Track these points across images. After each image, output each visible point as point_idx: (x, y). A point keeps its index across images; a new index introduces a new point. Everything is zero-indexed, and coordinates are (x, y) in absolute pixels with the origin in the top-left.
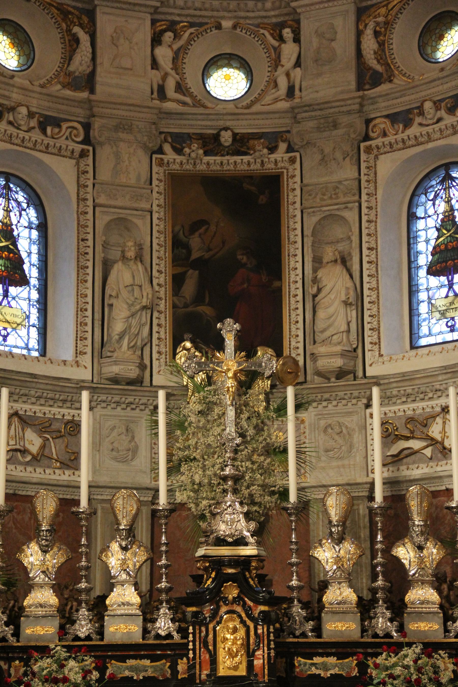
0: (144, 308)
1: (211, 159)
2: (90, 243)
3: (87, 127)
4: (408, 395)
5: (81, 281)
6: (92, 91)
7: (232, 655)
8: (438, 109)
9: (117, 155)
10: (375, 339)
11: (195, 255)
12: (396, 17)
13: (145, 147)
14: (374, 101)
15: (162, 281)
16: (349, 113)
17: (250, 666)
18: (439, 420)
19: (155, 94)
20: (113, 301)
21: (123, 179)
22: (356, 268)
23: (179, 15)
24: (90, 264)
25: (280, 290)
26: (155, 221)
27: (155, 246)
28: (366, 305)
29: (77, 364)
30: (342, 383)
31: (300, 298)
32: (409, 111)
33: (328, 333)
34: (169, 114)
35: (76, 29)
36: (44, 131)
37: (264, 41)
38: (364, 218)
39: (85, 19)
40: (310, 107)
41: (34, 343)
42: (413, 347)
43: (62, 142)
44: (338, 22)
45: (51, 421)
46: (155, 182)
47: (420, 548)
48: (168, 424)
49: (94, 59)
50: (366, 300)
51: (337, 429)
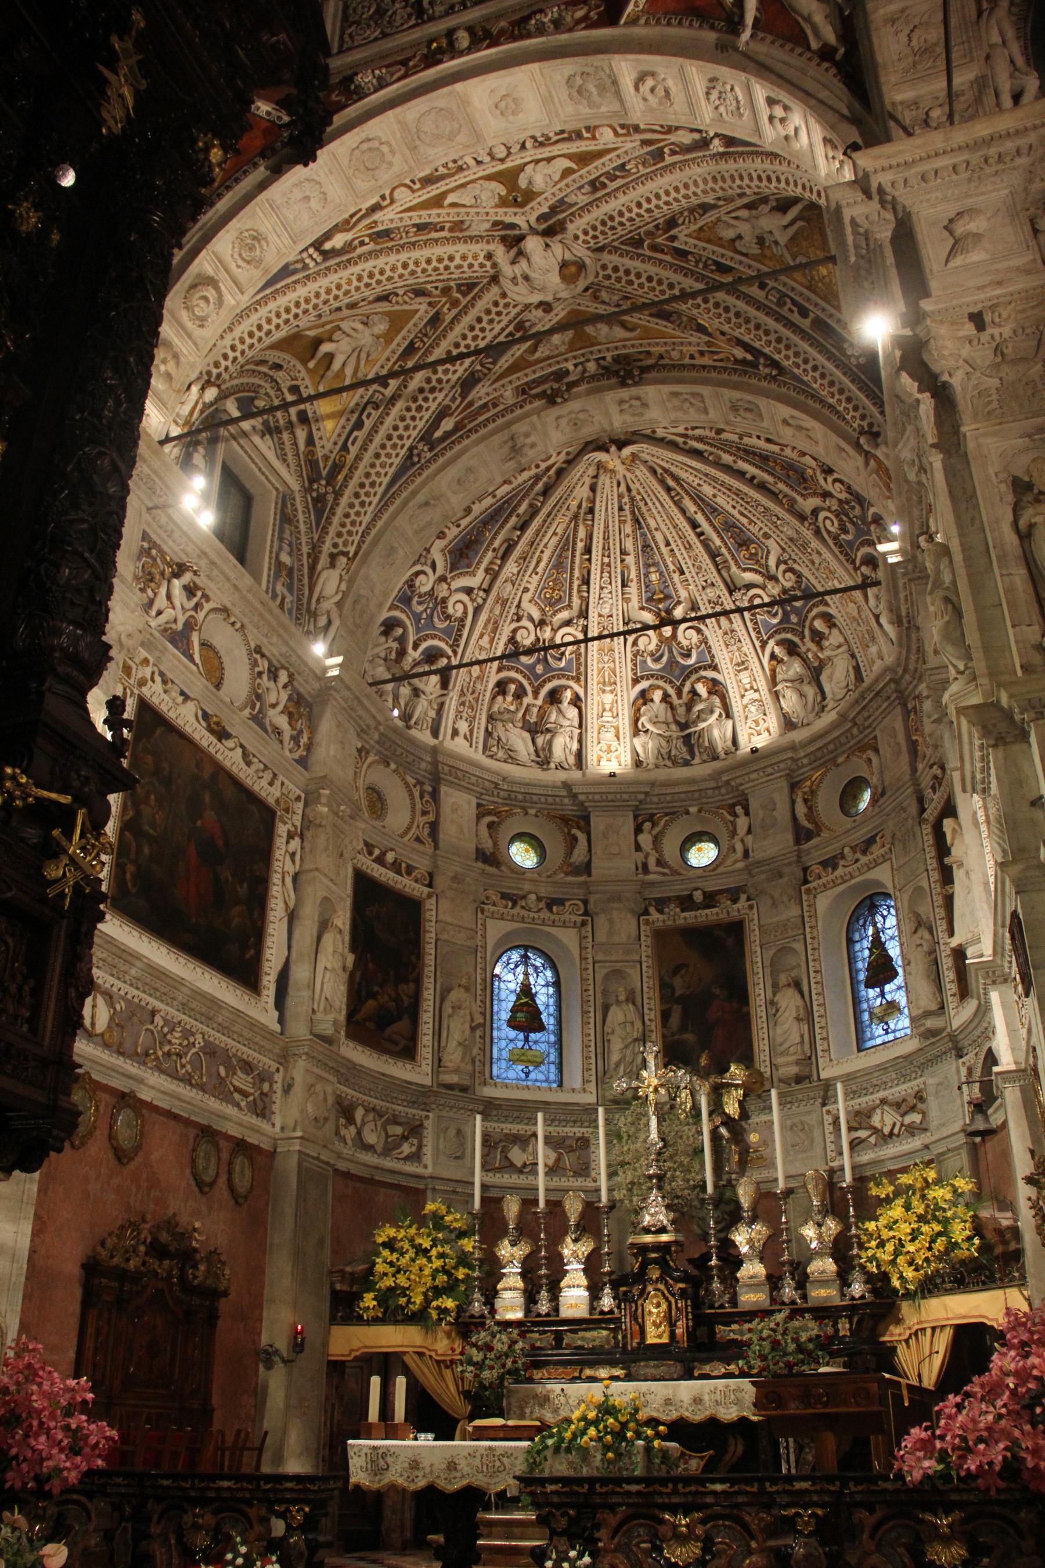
0: (636, 1040)
1: (687, 914)
2: (591, 992)
3: (585, 902)
4: (854, 1092)
5: (585, 1023)
6: (589, 874)
7: (657, 1326)
8: (855, 852)
9: (611, 921)
10: (825, 1047)
11: (678, 993)
12: (818, 786)
13: (633, 912)
14: (808, 852)
15: (652, 1016)
16: (789, 864)
17: (672, 1334)
18: (878, 1111)
20: (611, 1037)
21: (616, 939)
22: (805, 988)
24: (592, 1009)
25: (748, 1014)
26: (644, 968)
27: (645, 989)
28: (816, 1019)
29: (584, 1090)
30: (798, 1087)
31: (764, 1019)
32: (835, 857)
33: (786, 1045)
34: (652, 884)
35: (574, 831)
36: (551, 911)
37: (723, 819)
38: (809, 947)
39: (582, 823)
40: (759, 863)
41: (552, 1077)
42: (860, 1050)
43: (566, 917)
44: (777, 796)
45: (564, 1139)
46: (643, 938)
47: (820, 1225)
48: (607, 1135)
49: (590, 850)
50: (816, 1015)
51: (800, 1127)
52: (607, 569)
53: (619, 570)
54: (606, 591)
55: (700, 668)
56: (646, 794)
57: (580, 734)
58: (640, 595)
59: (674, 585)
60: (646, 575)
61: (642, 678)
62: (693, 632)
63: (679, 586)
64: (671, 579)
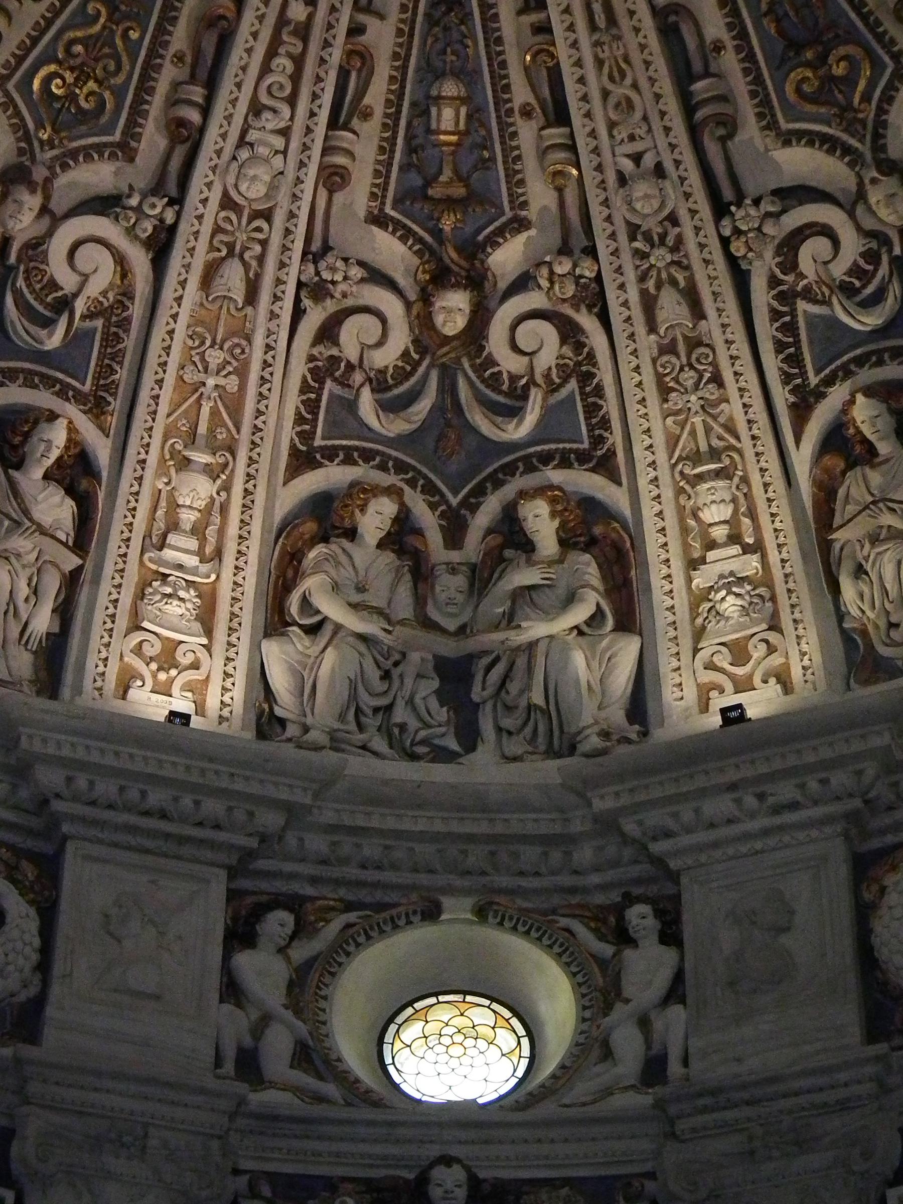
19: (229, 1067)
23: (314, 880)
39: (29, 871)
49: (44, 966)
52: (292, 44)
53: (336, 56)
54: (270, 122)
56: (290, 810)
57: (72, 580)
58: (382, 173)
59: (513, 158)
60: (421, 110)
62: (548, 331)
63: (530, 165)
64: (508, 135)
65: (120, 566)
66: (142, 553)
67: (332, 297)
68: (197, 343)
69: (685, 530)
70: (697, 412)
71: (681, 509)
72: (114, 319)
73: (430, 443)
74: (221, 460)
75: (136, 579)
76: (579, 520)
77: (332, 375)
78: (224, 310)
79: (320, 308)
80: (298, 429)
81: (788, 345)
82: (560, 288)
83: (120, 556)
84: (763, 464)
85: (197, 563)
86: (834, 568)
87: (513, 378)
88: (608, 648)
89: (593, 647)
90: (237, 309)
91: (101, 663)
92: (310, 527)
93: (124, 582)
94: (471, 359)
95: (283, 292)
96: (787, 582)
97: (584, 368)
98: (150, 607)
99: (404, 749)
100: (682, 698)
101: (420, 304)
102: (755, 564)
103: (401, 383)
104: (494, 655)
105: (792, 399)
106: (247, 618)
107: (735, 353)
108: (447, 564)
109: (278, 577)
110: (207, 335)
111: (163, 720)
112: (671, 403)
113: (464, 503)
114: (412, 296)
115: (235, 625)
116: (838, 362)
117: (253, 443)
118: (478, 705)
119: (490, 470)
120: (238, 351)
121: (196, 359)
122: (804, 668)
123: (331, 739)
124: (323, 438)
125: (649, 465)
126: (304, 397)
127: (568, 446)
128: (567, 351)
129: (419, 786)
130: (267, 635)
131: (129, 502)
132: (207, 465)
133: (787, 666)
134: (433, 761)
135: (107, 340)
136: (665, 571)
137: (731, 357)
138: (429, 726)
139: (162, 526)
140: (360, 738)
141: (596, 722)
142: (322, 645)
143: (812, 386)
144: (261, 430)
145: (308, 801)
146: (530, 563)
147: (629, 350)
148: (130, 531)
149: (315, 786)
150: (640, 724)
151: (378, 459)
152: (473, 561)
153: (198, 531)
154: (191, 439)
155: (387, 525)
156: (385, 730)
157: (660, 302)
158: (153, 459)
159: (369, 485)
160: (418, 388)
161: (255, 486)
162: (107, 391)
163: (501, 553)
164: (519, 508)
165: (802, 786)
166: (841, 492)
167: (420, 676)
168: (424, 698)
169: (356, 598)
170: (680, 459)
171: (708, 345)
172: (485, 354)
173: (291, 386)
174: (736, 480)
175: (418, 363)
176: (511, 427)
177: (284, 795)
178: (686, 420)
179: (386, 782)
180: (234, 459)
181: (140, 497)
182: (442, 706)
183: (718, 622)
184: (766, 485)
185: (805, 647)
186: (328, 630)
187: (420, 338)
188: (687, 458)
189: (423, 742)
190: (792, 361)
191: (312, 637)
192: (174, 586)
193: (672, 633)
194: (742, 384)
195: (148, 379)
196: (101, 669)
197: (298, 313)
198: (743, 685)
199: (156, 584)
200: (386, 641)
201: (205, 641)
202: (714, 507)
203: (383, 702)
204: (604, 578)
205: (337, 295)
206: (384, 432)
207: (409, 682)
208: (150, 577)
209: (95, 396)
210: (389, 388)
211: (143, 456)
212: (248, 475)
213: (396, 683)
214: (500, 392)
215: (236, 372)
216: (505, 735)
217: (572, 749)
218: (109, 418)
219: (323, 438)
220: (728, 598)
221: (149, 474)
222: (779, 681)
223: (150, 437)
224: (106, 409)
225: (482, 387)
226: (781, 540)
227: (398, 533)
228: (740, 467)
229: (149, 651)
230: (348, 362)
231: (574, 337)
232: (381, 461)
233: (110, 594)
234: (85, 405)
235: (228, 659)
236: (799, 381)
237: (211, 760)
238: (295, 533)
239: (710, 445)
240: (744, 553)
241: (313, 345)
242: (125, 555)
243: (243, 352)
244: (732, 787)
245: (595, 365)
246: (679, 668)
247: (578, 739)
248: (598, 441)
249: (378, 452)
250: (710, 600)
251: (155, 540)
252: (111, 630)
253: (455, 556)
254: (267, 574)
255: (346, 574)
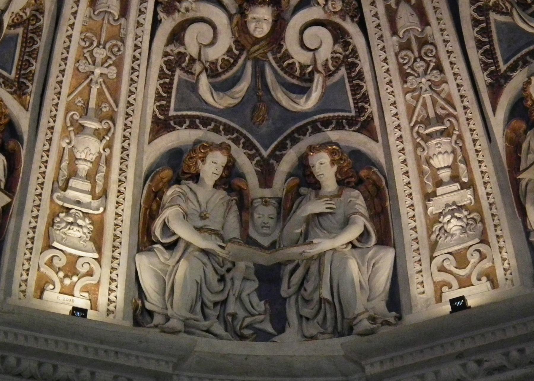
55: (326, 123)
61: (180, 121)
65: (37, 202)
66: (52, 192)
67: (179, 11)
68: (87, 44)
69: (421, 173)
70: (426, 90)
71: (418, 159)
72: (31, 27)
73: (248, 112)
74: (106, 127)
75: (48, 212)
76: (350, 167)
77: (180, 65)
78: (106, 21)
79: (170, 19)
80: (158, 104)
81: (484, 43)
82: (332, 4)
83: (37, 195)
84: (472, 126)
85: (90, 200)
86: (522, 199)
87: (303, 67)
88: (372, 257)
89: (362, 256)
90: (115, 20)
91: (24, 273)
92: (167, 173)
93: (40, 214)
94: (273, 54)
95: (146, 8)
96: (491, 209)
97: (350, 60)
98: (58, 232)
99: (235, 333)
100: (424, 293)
101: (239, 15)
102: (469, 196)
103: (227, 71)
104: (295, 264)
105: (489, 81)
106: (125, 239)
107: (450, 49)
108: (262, 198)
109: (146, 209)
110: (94, 39)
111: (68, 313)
112: (409, 84)
113: (272, 155)
114: (233, 11)
115: (117, 244)
116: (519, 55)
117: (127, 114)
118: (285, 299)
119: (289, 131)
120: (116, 49)
121: (87, 55)
122: (504, 269)
123: (185, 325)
124: (175, 110)
125: (396, 127)
126: (162, 82)
127: (341, 114)
128: (338, 48)
129: (246, 359)
130: (139, 251)
131: (42, 156)
132: (96, 130)
133: (493, 268)
134: (255, 340)
135: (26, 42)
136: (409, 202)
137: (448, 52)
138: (253, 315)
139: (66, 173)
140: (205, 324)
141: (367, 310)
142: (177, 258)
143: (502, 71)
144: (133, 105)
145: (170, 370)
146: (318, 197)
147: (380, 47)
148: (44, 178)
149: (175, 360)
150: (397, 312)
151: (213, 124)
152: (279, 196)
153: (90, 177)
154: (85, 111)
155: (220, 171)
156: (222, 318)
157: (399, 14)
158: (58, 126)
159: (207, 143)
160: (239, 74)
161: (129, 144)
162: (26, 78)
163: (298, 190)
164: (310, 158)
165: (507, 355)
166: (525, 146)
167: (245, 279)
168: (249, 295)
169: (200, 223)
170: (416, 123)
171: (432, 44)
172: (283, 50)
173: (152, 73)
174: (454, 137)
175: (239, 57)
176: (302, 101)
177: (152, 366)
178: (420, 95)
179: (224, 356)
180: (114, 125)
181: (51, 153)
182: (261, 300)
183: (446, 237)
184: (475, 141)
185: (505, 255)
186: (181, 246)
187: (239, 39)
188: (421, 122)
189: (248, 327)
190: (488, 54)
191: (171, 251)
192: (75, 217)
193: (415, 246)
194: (456, 71)
195: (54, 70)
196: (24, 277)
197: (156, 23)
198: (465, 283)
199: (62, 215)
200: (221, 254)
201: (96, 256)
202: (440, 156)
203: (220, 298)
204: (369, 207)
205: (183, 10)
206: (217, 105)
207: (237, 283)
208: (57, 209)
209: (18, 82)
210: (218, 75)
211: (52, 124)
212: (124, 136)
213: (229, 284)
214: (294, 77)
215: (114, 64)
216: (304, 320)
217: (350, 330)
218: (28, 97)
219: (175, 110)
220: (452, 221)
221: (56, 136)
222: (489, 279)
223: (56, 110)
224: (25, 91)
225: (281, 73)
226: (486, 179)
227: (228, 177)
228: (456, 128)
229: (58, 263)
230: (191, 56)
231: (342, 38)
232: (215, 126)
233: (30, 223)
234: (11, 88)
235: (113, 268)
236: (493, 68)
237: (102, 342)
238: (158, 177)
239: (436, 113)
240: (462, 188)
241: (167, 45)
242: (40, 195)
243: (119, 50)
244: (460, 356)
245: (357, 57)
246: (421, 271)
247: (354, 323)
248: (361, 110)
249: (212, 120)
250: (440, 222)
251: (61, 183)
252: (31, 249)
253: (267, 193)
254: (138, 208)
255: (193, 206)
